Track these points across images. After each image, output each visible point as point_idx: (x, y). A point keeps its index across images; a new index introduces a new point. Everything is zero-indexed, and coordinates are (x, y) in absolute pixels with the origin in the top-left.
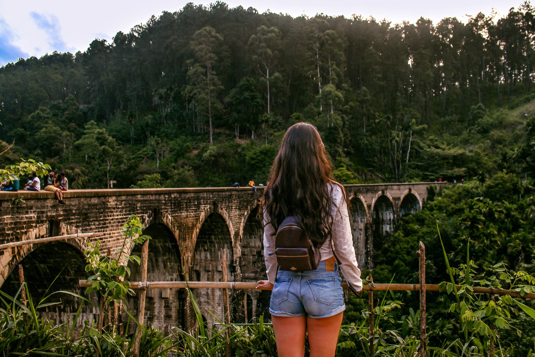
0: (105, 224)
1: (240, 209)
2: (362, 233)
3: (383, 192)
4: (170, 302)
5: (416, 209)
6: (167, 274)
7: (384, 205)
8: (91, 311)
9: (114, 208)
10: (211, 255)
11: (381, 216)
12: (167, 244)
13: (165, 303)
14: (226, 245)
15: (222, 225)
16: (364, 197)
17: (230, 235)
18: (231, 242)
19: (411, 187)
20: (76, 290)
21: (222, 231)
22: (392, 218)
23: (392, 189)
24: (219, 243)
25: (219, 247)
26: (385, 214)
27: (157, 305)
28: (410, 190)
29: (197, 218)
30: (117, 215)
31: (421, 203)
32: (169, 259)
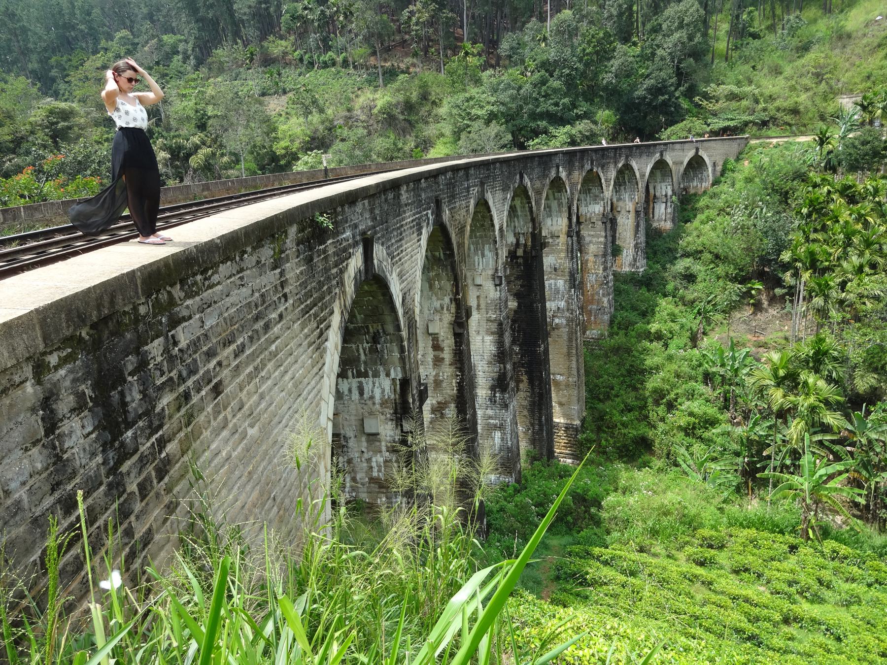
0: (401, 234)
1: (503, 190)
2: (632, 215)
3: (662, 155)
4: (441, 339)
5: (702, 179)
6: (434, 298)
8: (388, 375)
9: (406, 205)
11: (652, 191)
12: (437, 254)
13: (433, 340)
14: (487, 247)
15: (483, 217)
16: (637, 163)
17: (494, 231)
18: (496, 242)
19: (699, 145)
20: (362, 344)
21: (483, 225)
22: (670, 193)
23: (673, 150)
25: (476, 250)
26: (658, 187)
27: (421, 344)
28: (697, 149)
30: (409, 217)
31: (710, 169)
32: (438, 275)
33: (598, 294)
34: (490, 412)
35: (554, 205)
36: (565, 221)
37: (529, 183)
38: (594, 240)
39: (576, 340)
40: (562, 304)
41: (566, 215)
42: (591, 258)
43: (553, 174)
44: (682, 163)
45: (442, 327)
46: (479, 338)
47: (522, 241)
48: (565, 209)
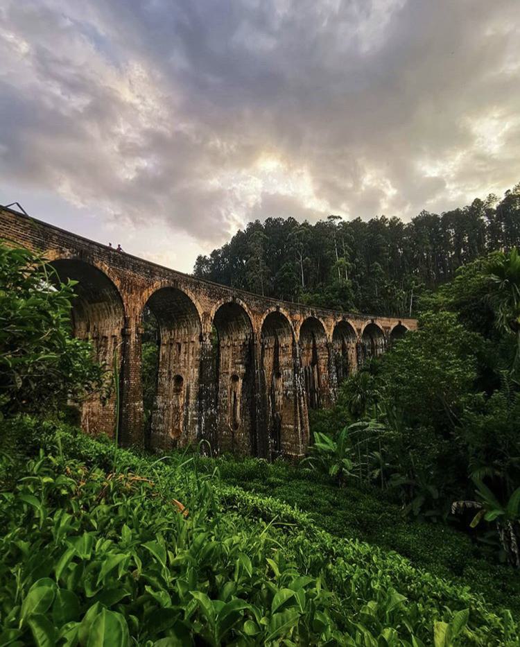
2: (354, 350)
7: (376, 333)
10: (188, 330)
11: (375, 342)
17: (198, 313)
24: (192, 320)
27: (109, 343)
28: (400, 322)
29: (151, 284)
33: (327, 386)
34: (194, 413)
35: (285, 330)
36: (292, 338)
37: (245, 306)
38: (323, 357)
39: (300, 404)
40: (291, 383)
41: (291, 335)
42: (323, 367)
43: (273, 309)
44: (389, 328)
45: (117, 332)
46: (192, 370)
47: (249, 337)
48: (290, 332)
